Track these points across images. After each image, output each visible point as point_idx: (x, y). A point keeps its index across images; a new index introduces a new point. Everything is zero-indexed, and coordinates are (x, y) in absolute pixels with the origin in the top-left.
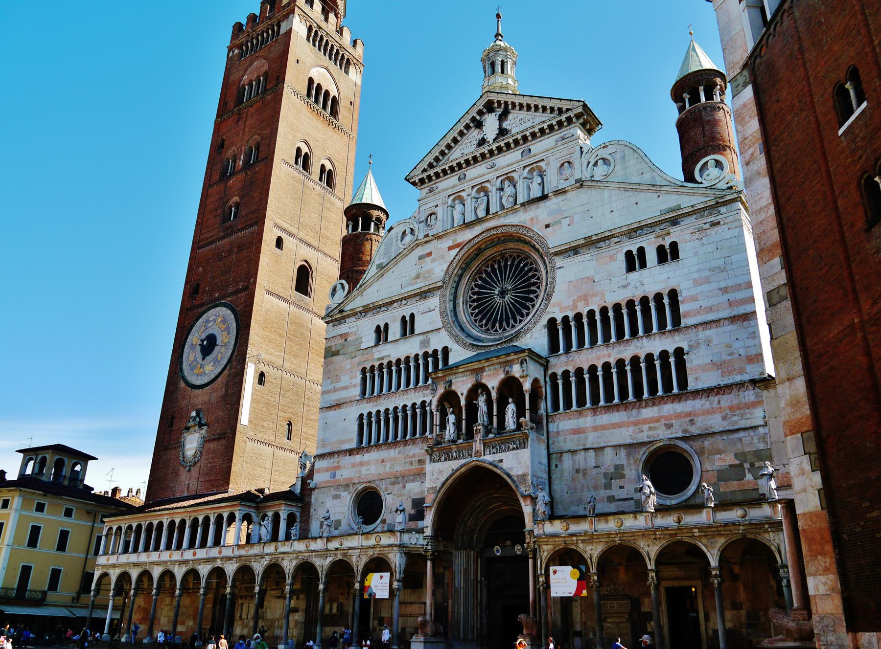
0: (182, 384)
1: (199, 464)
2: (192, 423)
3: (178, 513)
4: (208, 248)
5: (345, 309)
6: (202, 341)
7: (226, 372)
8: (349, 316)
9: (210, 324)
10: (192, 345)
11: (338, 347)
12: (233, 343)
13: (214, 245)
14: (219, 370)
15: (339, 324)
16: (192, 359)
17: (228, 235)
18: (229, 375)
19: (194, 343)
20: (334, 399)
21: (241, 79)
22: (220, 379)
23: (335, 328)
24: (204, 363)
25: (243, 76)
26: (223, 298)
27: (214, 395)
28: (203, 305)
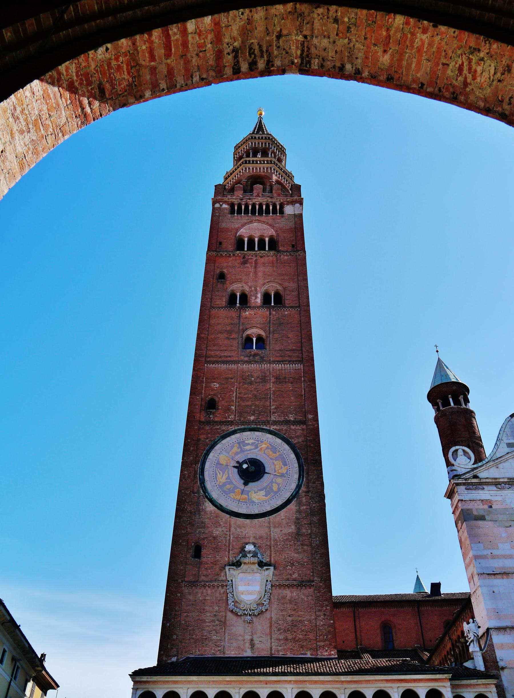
0: (209, 507)
1: (268, 615)
2: (249, 559)
3: (316, 682)
4: (224, 366)
5: (481, 475)
6: (240, 464)
7: (292, 506)
8: (488, 484)
9: (248, 447)
10: (219, 463)
11: (482, 513)
12: (296, 476)
13: (233, 367)
14: (280, 503)
15: (476, 489)
16: (222, 478)
17: (249, 362)
18: (299, 511)
19: (223, 462)
20: (496, 565)
21: (237, 230)
22: (282, 513)
23: (470, 491)
24: (247, 488)
25: (240, 228)
26: (267, 423)
27: (277, 530)
28: (231, 423)
